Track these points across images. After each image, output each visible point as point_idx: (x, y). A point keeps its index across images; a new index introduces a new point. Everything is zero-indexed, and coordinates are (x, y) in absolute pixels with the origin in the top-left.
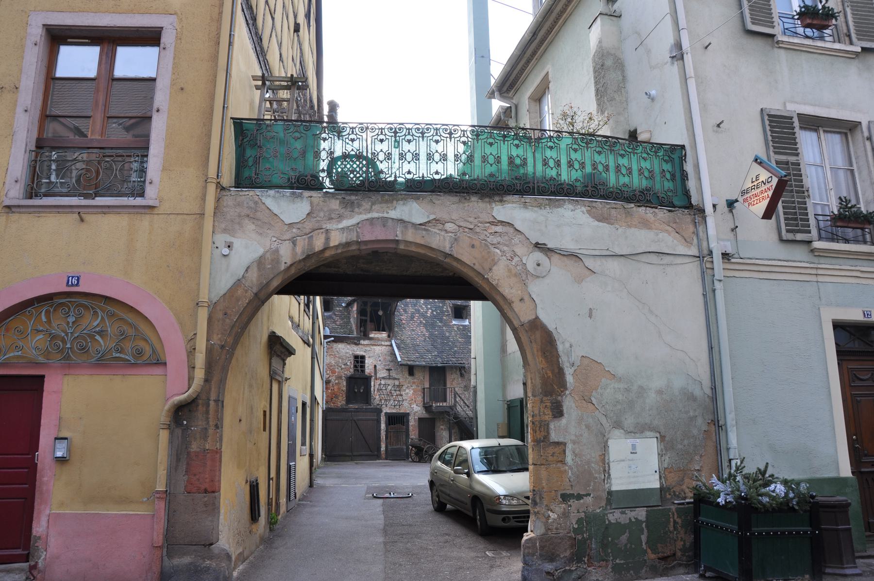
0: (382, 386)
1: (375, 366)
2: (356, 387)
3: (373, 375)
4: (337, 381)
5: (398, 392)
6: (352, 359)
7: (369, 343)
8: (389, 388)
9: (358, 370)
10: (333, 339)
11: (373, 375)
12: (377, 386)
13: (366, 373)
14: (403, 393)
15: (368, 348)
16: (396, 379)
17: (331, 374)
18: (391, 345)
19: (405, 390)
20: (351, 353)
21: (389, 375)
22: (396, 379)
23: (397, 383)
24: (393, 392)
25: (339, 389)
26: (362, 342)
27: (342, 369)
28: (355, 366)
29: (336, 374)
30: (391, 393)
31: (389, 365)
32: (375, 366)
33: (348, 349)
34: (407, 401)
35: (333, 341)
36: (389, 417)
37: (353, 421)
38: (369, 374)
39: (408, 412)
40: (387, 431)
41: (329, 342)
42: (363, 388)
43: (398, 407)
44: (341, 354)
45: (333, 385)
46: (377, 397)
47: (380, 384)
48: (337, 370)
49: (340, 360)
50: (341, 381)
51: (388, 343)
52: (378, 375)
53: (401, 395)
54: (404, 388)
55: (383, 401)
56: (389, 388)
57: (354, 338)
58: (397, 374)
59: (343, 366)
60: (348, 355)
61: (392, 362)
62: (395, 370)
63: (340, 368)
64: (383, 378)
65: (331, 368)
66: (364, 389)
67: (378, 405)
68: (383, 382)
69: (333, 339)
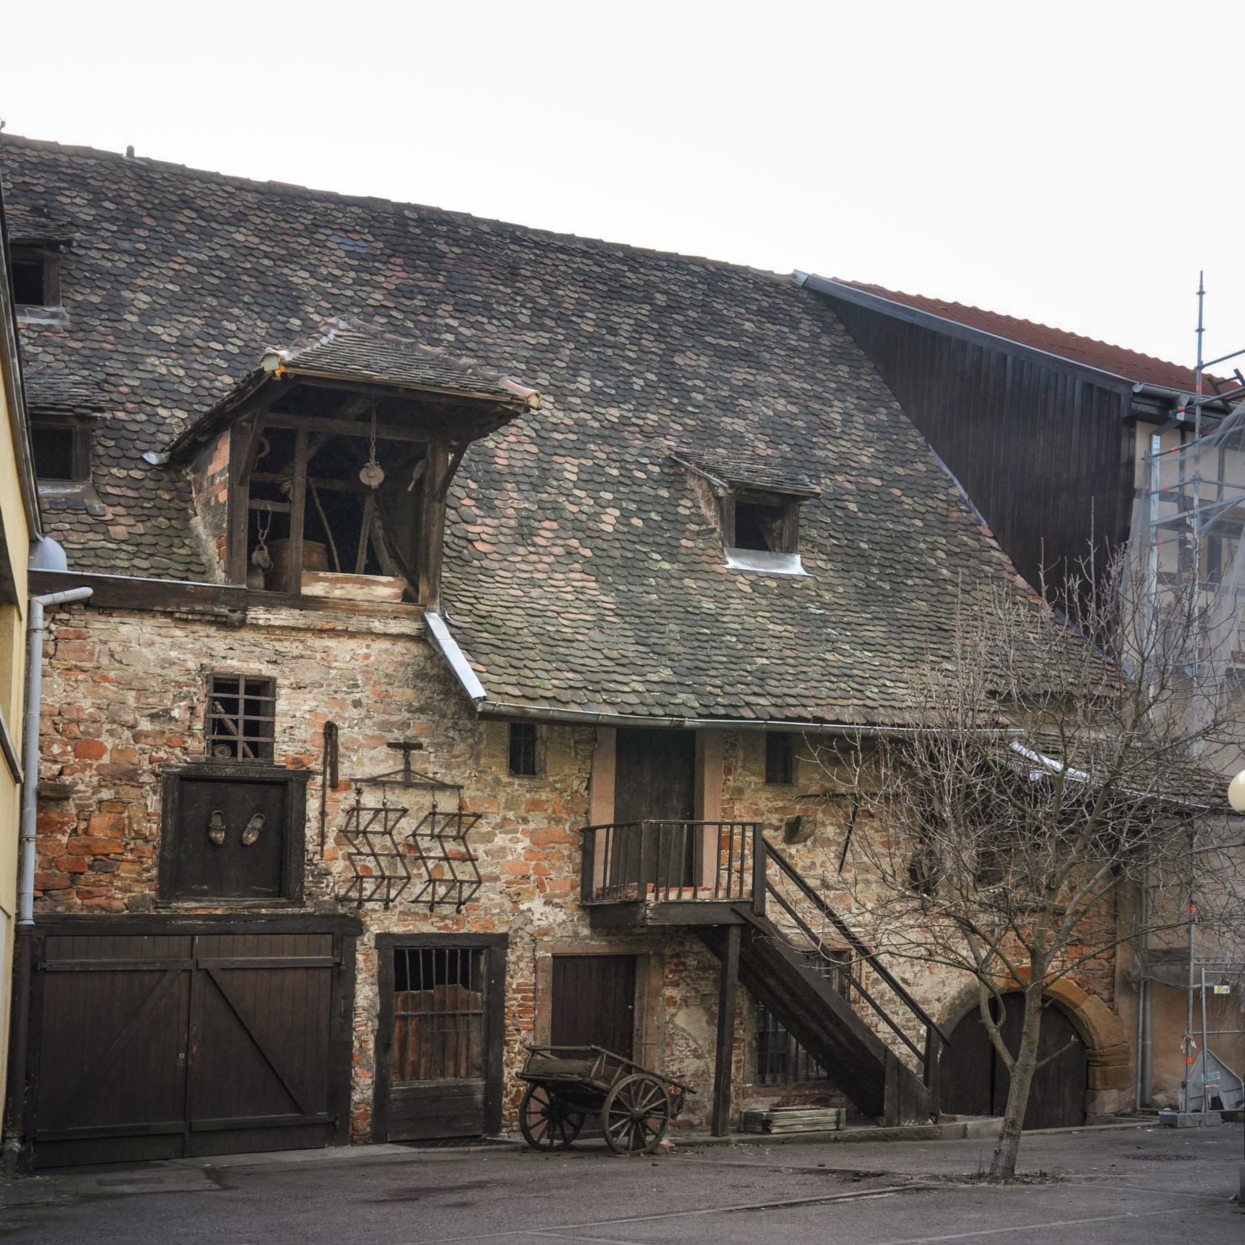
0: (366, 817)
1: (330, 730)
2: (217, 821)
3: (316, 766)
4: (106, 794)
5: (450, 846)
6: (200, 694)
7: (301, 623)
8: (406, 826)
9: (233, 746)
10: (87, 591)
11: (316, 766)
12: (337, 819)
13: (279, 760)
14: (479, 850)
15: (291, 647)
16: (443, 786)
17: (71, 758)
18: (425, 637)
19: (488, 838)
20: (192, 664)
21: (407, 770)
22: (443, 786)
23: (447, 804)
24: (424, 843)
25: (118, 827)
26: (259, 615)
27: (137, 737)
28: (217, 726)
29: (106, 759)
30: (415, 847)
31: (405, 725)
32: (330, 730)
33: (181, 647)
34: (500, 885)
35: (87, 604)
36: (399, 955)
37: (197, 976)
38: (296, 761)
39: (503, 929)
40: (385, 1017)
41: (64, 606)
42: (258, 824)
43: (448, 910)
44: (139, 668)
45: (81, 808)
46: (338, 866)
47: (356, 809)
48: (108, 742)
49: (131, 697)
50: (129, 792)
51: (408, 627)
52: (345, 771)
53: (471, 859)
54: (484, 827)
55: (369, 886)
56: (406, 826)
57: (214, 596)
58: (448, 766)
59: (145, 725)
60: (173, 673)
61: (422, 710)
62: (438, 746)
63: (127, 734)
64: (375, 782)
65: (76, 730)
66: (262, 833)
67: (340, 900)
68: (371, 799)
69: (87, 591)
